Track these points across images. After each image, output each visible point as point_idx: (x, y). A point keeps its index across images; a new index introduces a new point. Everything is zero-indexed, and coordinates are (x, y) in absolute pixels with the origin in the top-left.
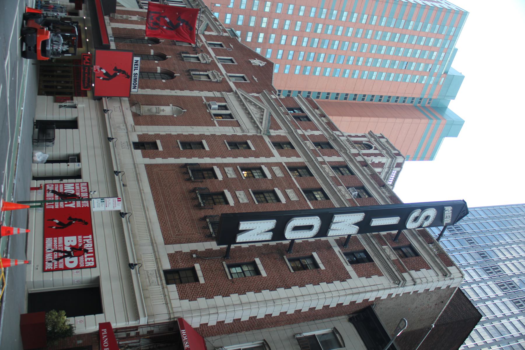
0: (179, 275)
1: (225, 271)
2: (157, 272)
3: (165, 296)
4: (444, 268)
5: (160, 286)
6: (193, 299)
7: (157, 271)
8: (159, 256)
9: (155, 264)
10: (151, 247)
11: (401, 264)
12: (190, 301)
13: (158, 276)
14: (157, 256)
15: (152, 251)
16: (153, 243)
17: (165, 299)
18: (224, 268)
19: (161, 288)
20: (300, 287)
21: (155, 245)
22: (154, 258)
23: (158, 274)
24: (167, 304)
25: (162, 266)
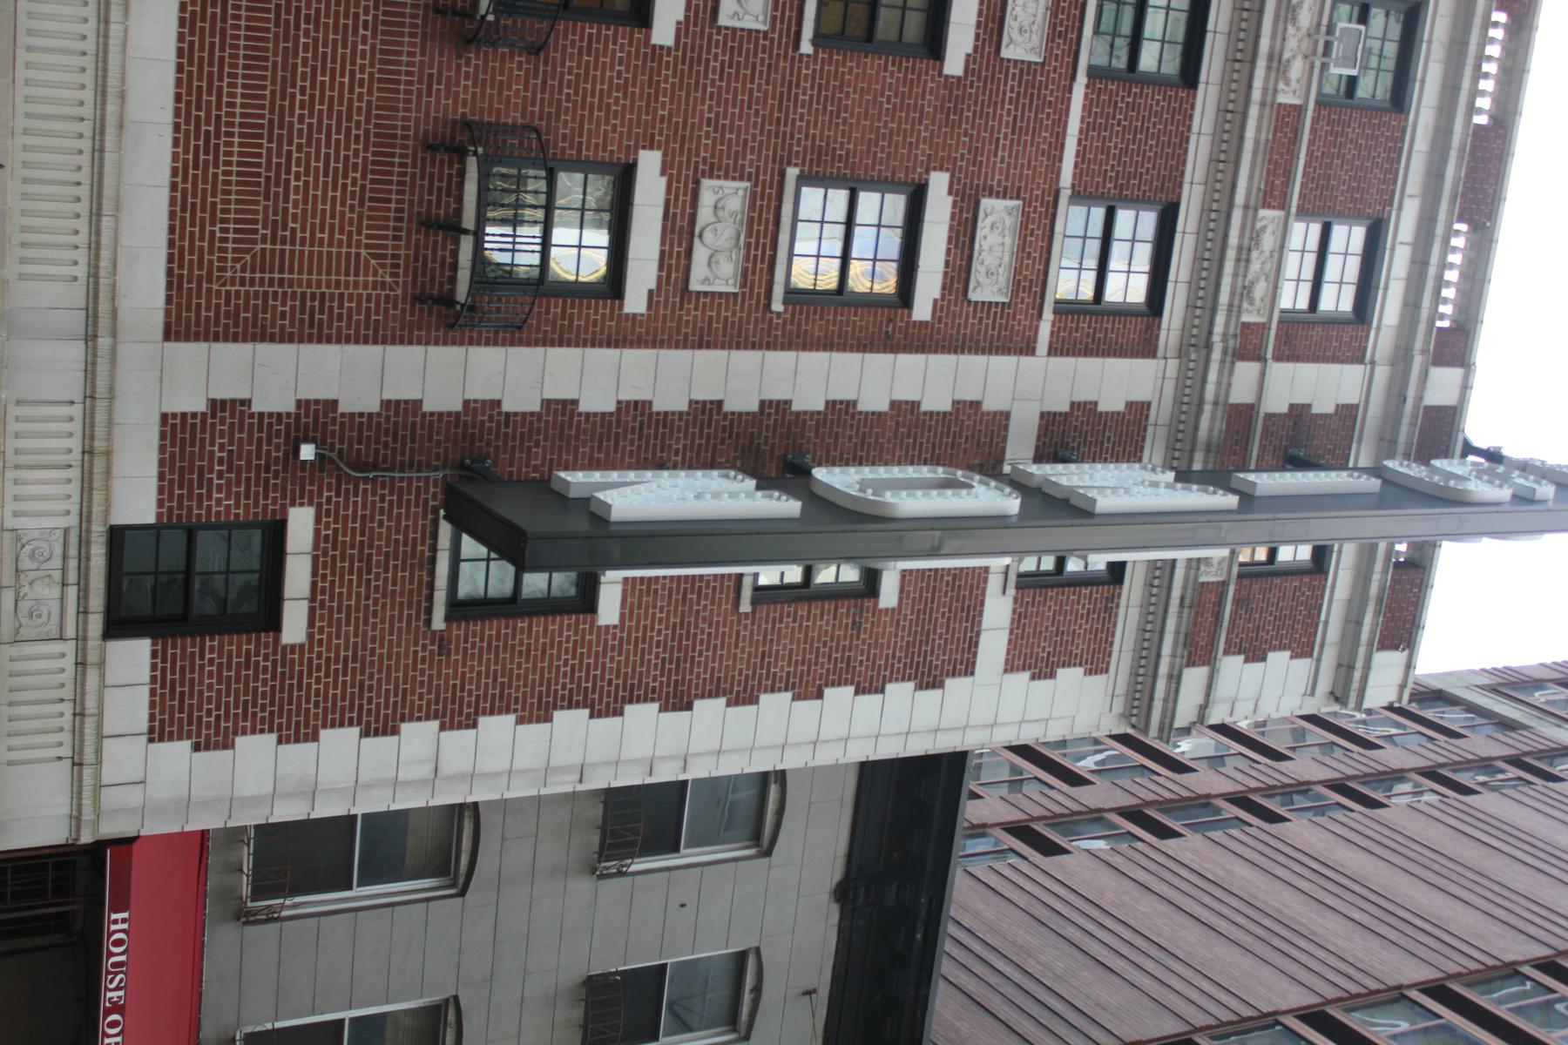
0: (180, 593)
1: (432, 573)
2: (73, 552)
3: (79, 714)
4: (1418, 360)
5: (69, 648)
6: (213, 738)
7: (73, 539)
8: (109, 437)
9: (74, 489)
10: (77, 351)
11: (1218, 616)
12: (196, 748)
13: (72, 576)
14: (100, 431)
15: (72, 385)
16: (96, 323)
17: (77, 733)
18: (434, 549)
19: (68, 663)
20: (734, 702)
21: (104, 342)
22: (76, 444)
23: (73, 564)
24: (77, 764)
25: (107, 502)
